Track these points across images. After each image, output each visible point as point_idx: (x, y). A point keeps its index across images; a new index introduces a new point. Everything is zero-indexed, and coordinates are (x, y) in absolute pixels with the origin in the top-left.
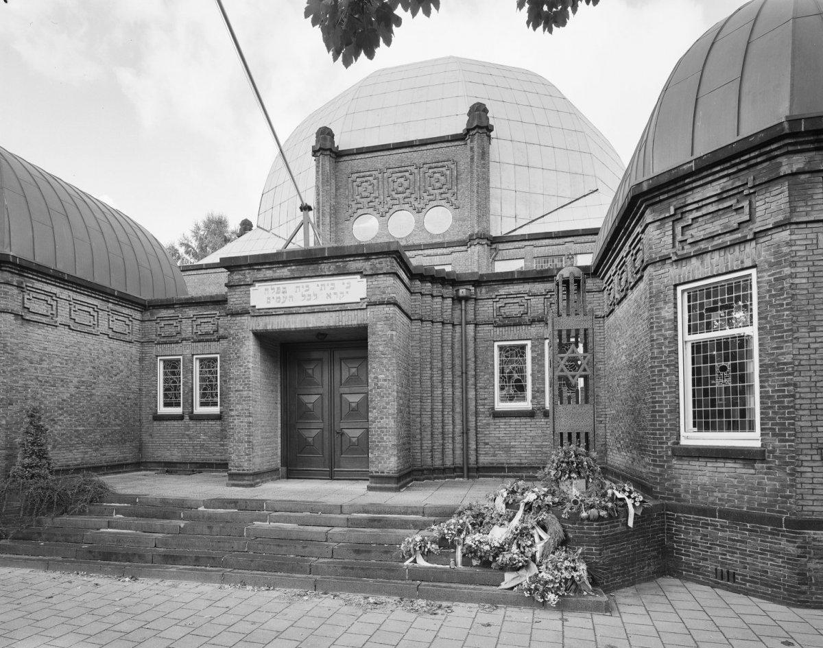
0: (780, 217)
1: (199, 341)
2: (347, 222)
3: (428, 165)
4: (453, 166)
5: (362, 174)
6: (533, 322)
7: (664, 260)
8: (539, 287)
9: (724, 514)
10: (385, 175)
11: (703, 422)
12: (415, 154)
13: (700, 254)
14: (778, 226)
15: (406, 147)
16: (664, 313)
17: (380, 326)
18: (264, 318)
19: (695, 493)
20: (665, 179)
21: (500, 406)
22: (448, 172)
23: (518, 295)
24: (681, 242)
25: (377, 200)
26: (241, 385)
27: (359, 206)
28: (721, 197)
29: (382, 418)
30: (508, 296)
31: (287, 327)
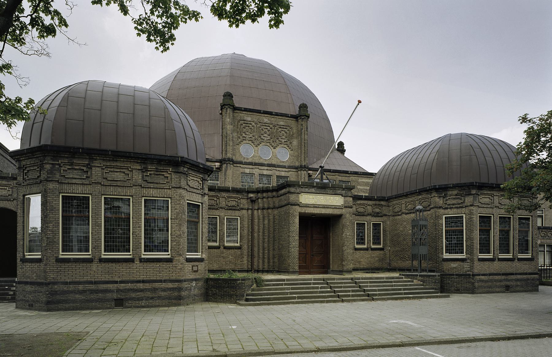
0: (471, 204)
1: (230, 209)
2: (238, 146)
3: (279, 126)
4: (290, 130)
5: (246, 122)
6: (368, 215)
7: (440, 207)
8: (370, 202)
9: (456, 275)
10: (258, 125)
11: (448, 251)
12: (273, 119)
13: (451, 208)
14: (471, 205)
15: (268, 114)
16: (440, 222)
17: (348, 215)
18: (304, 208)
19: (449, 270)
20: (443, 186)
21: (357, 246)
22: (288, 132)
23: (363, 204)
24: (445, 203)
25: (254, 138)
26: (295, 234)
27: (244, 138)
28: (456, 195)
29: (348, 249)
30: (360, 204)
31: (314, 212)
